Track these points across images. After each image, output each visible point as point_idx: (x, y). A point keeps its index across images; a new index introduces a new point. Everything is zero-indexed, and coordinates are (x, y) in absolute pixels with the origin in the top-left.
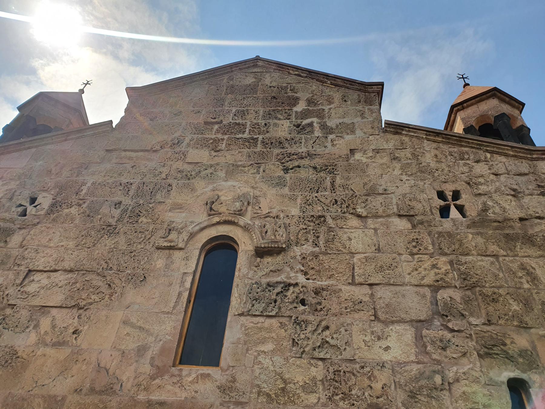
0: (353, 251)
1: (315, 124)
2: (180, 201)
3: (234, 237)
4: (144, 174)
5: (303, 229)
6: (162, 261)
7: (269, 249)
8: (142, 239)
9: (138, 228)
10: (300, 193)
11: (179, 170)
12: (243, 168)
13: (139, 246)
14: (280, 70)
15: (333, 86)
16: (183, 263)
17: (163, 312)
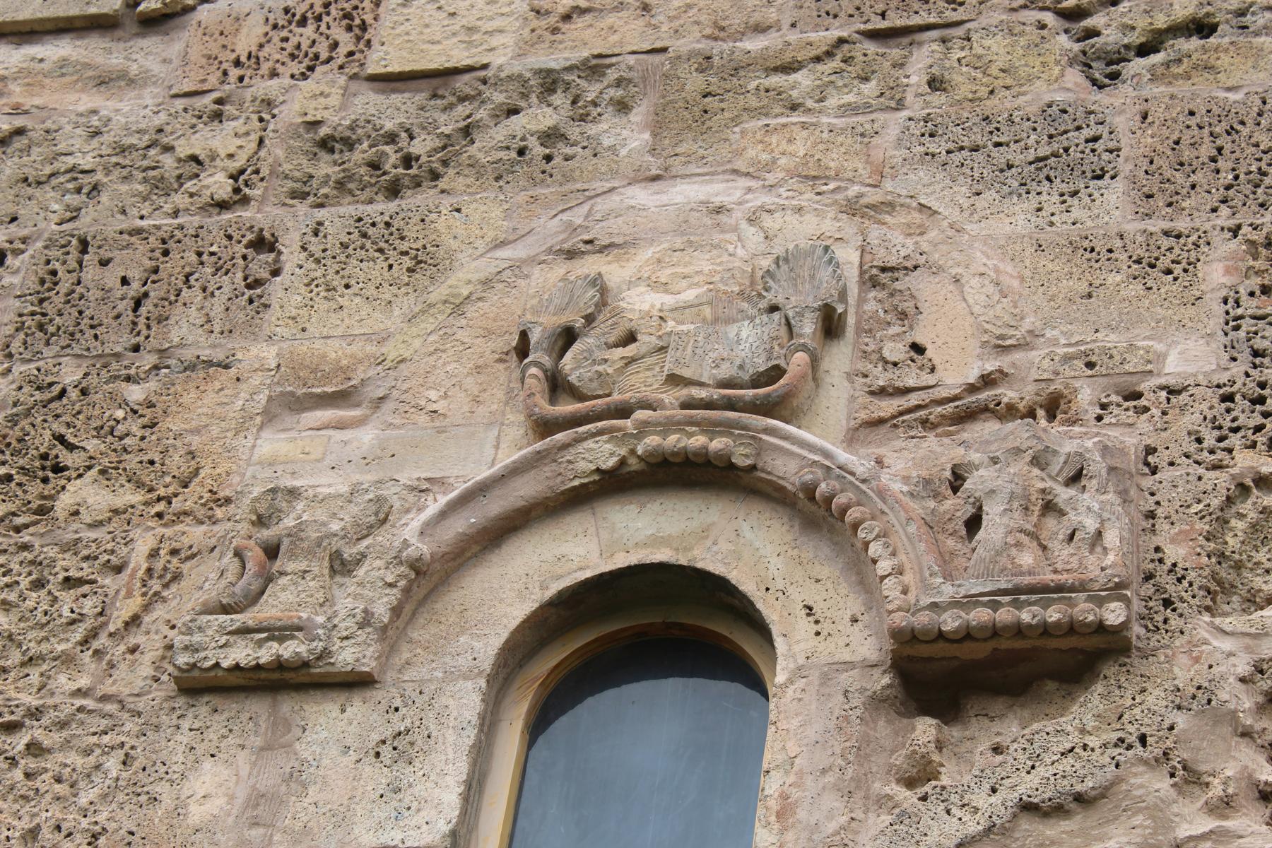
2: (335, 351)
3: (734, 577)
4: (86, 180)
6: (225, 772)
7: (1005, 644)
8: (79, 633)
9: (52, 552)
10: (1224, 217)
11: (324, 131)
12: (776, 80)
13: (63, 682)
16: (376, 776)
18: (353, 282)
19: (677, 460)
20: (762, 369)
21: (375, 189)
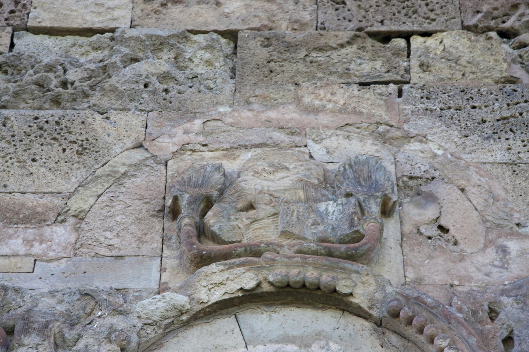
18: (37, 158)
19: (297, 286)
20: (348, 232)
21: (43, 100)
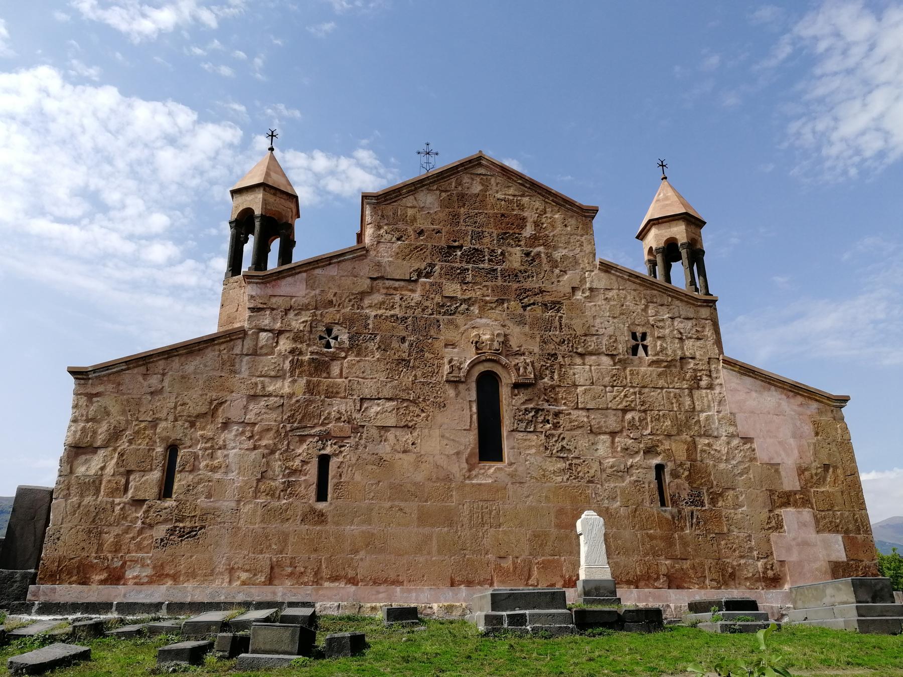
0: (577, 384)
1: (543, 255)
5: (544, 366)
10: (538, 332)
14: (504, 175)
15: (554, 204)
16: (467, 393)
17: (465, 430)
